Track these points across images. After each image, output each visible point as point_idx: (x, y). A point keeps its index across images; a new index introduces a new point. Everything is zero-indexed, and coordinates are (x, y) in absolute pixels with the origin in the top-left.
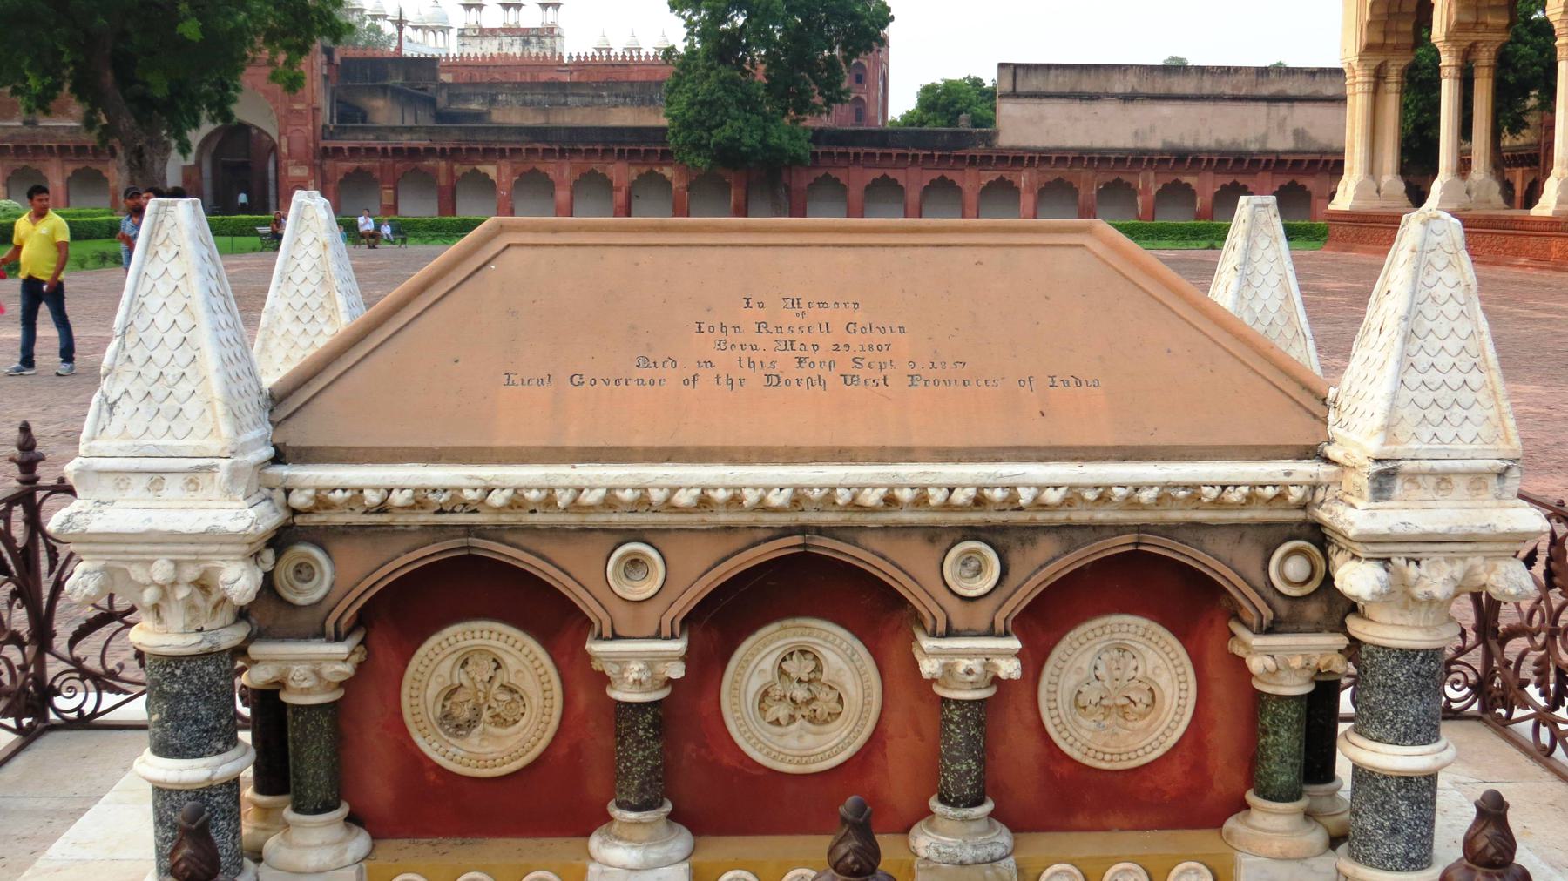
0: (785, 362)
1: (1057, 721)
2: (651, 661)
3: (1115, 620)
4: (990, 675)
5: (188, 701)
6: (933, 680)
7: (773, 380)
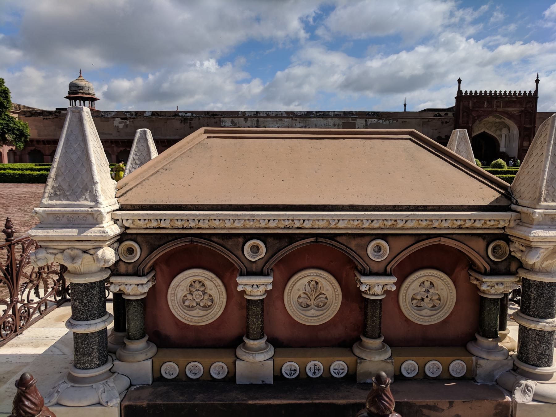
6: (363, 292)
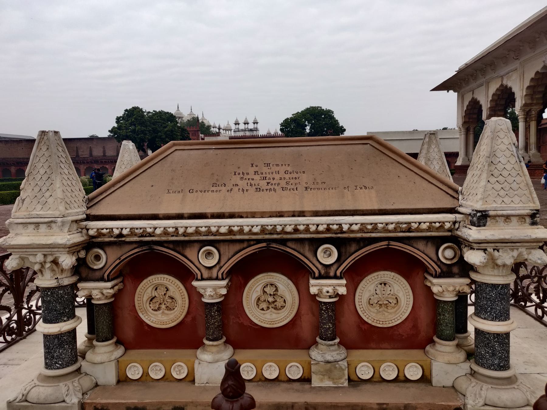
1: (362, 309)
2: (215, 289)
3: (382, 273)
4: (336, 293)
5: (53, 303)
7: (258, 190)
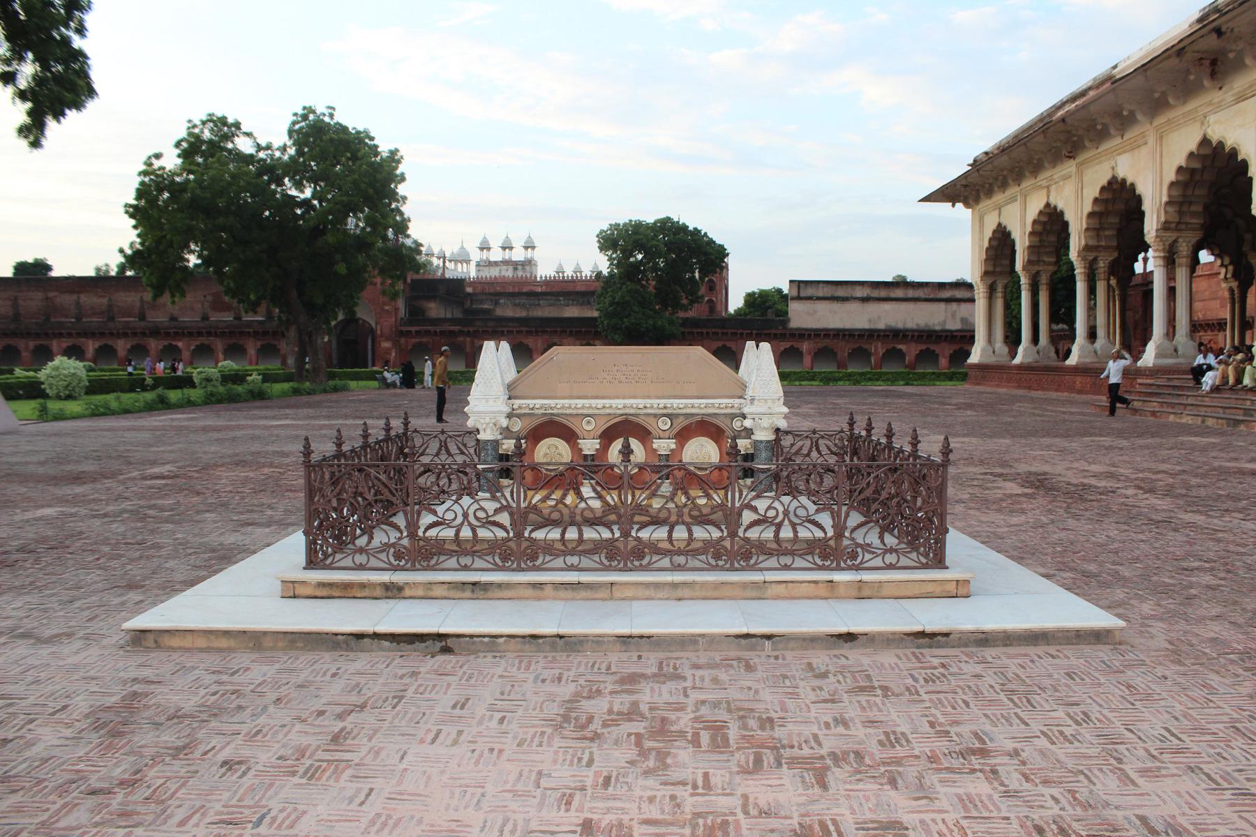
0: (623, 378)
